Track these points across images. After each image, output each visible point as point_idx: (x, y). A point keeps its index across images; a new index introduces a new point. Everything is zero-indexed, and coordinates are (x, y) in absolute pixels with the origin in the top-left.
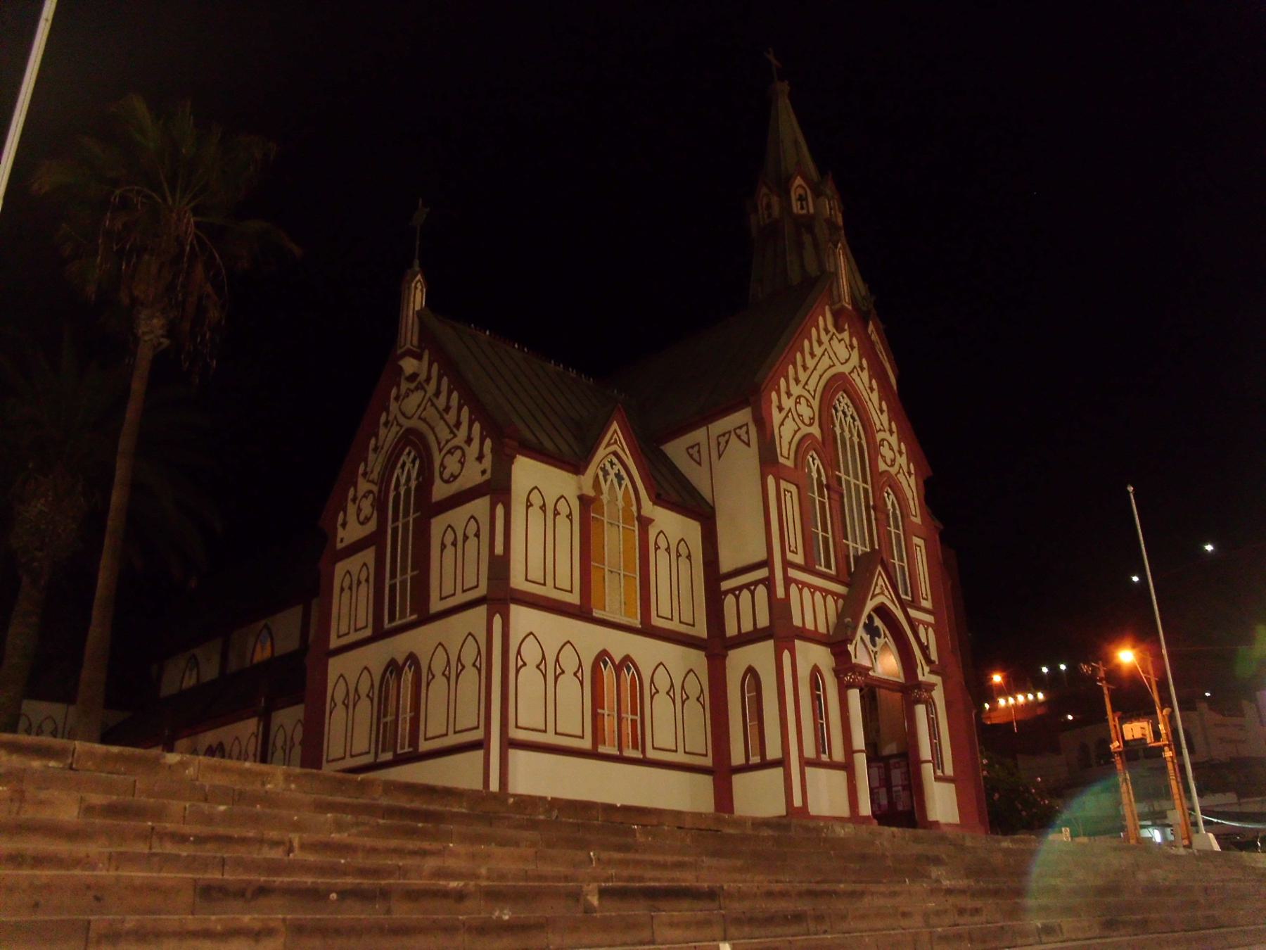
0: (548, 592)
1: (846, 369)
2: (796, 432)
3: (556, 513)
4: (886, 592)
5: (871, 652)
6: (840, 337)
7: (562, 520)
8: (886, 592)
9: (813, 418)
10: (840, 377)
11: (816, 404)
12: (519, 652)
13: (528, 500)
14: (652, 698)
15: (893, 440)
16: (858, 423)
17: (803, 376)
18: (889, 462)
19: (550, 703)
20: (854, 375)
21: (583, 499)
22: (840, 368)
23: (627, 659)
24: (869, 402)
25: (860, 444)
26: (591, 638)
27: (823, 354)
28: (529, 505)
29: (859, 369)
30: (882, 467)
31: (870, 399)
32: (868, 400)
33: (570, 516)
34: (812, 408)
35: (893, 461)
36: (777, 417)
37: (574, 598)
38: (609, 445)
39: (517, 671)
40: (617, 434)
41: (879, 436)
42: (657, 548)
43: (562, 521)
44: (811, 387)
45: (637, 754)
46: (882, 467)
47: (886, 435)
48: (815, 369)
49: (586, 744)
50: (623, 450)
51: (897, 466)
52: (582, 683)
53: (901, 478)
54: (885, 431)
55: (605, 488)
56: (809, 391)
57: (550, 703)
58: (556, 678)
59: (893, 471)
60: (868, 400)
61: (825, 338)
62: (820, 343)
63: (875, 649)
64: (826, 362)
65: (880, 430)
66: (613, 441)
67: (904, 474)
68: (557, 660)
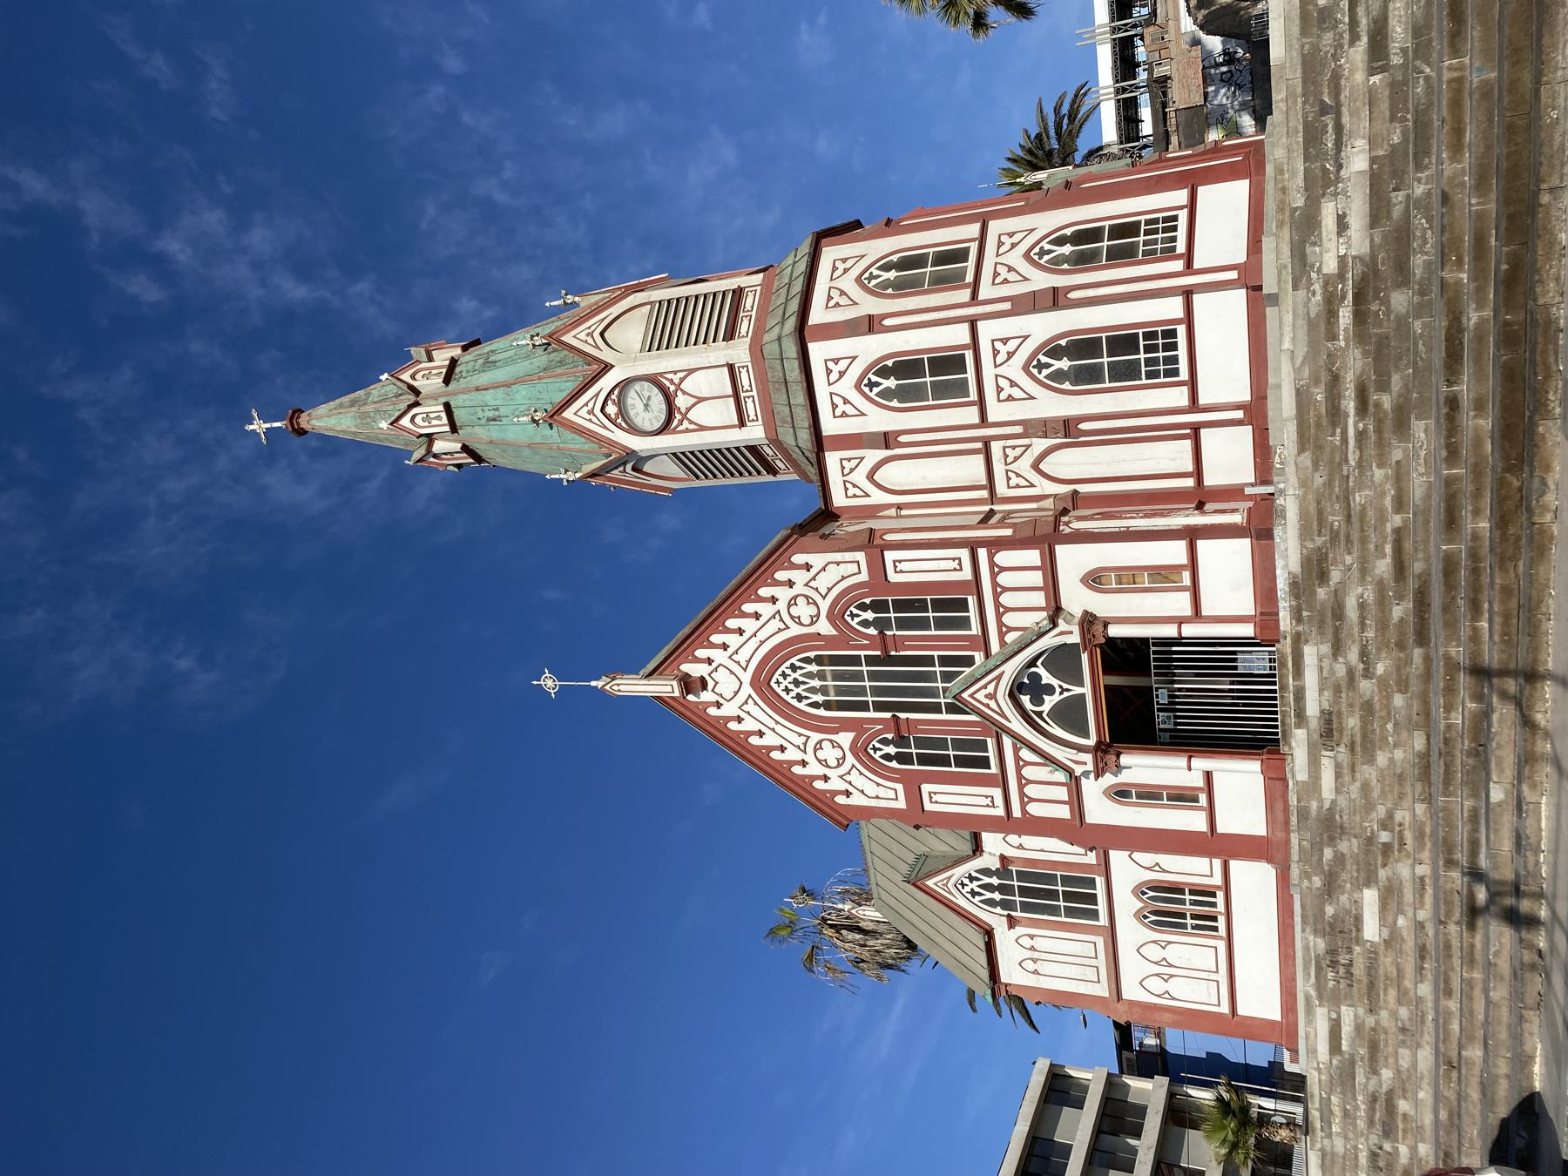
0: (1102, 962)
1: (747, 677)
2: (861, 773)
3: (1032, 949)
4: (991, 688)
5: (1062, 697)
6: (711, 684)
7: (1038, 943)
8: (991, 688)
9: (831, 741)
10: (755, 683)
11: (816, 737)
12: (1159, 996)
13: (1033, 973)
14: (1165, 871)
15: (783, 594)
16: (793, 660)
17: (792, 754)
18: (813, 610)
19: (1192, 974)
20: (742, 657)
21: (1012, 922)
22: (747, 690)
23: (1139, 891)
24: (761, 636)
25: (819, 660)
26: (1131, 932)
28: (1036, 972)
29: (730, 651)
30: (824, 627)
32: (754, 643)
33: (1032, 937)
34: (820, 742)
35: (810, 601)
36: (857, 800)
37: (1100, 941)
38: (950, 893)
39: (1174, 999)
40: (939, 882)
41: (795, 630)
42: (1021, 847)
43: (1038, 943)
44: (800, 741)
45: (1220, 895)
46: (824, 627)
47: (782, 605)
48: (773, 730)
49: (1222, 945)
50: (949, 878)
52: (1170, 943)
53: (823, 582)
55: (988, 895)
56: (805, 744)
57: (1192, 974)
58: (1171, 966)
59: (825, 606)
60: (754, 643)
61: (729, 710)
62: (739, 720)
63: (1058, 690)
64: (750, 707)
65: (781, 620)
66: (946, 888)
68: (1156, 963)
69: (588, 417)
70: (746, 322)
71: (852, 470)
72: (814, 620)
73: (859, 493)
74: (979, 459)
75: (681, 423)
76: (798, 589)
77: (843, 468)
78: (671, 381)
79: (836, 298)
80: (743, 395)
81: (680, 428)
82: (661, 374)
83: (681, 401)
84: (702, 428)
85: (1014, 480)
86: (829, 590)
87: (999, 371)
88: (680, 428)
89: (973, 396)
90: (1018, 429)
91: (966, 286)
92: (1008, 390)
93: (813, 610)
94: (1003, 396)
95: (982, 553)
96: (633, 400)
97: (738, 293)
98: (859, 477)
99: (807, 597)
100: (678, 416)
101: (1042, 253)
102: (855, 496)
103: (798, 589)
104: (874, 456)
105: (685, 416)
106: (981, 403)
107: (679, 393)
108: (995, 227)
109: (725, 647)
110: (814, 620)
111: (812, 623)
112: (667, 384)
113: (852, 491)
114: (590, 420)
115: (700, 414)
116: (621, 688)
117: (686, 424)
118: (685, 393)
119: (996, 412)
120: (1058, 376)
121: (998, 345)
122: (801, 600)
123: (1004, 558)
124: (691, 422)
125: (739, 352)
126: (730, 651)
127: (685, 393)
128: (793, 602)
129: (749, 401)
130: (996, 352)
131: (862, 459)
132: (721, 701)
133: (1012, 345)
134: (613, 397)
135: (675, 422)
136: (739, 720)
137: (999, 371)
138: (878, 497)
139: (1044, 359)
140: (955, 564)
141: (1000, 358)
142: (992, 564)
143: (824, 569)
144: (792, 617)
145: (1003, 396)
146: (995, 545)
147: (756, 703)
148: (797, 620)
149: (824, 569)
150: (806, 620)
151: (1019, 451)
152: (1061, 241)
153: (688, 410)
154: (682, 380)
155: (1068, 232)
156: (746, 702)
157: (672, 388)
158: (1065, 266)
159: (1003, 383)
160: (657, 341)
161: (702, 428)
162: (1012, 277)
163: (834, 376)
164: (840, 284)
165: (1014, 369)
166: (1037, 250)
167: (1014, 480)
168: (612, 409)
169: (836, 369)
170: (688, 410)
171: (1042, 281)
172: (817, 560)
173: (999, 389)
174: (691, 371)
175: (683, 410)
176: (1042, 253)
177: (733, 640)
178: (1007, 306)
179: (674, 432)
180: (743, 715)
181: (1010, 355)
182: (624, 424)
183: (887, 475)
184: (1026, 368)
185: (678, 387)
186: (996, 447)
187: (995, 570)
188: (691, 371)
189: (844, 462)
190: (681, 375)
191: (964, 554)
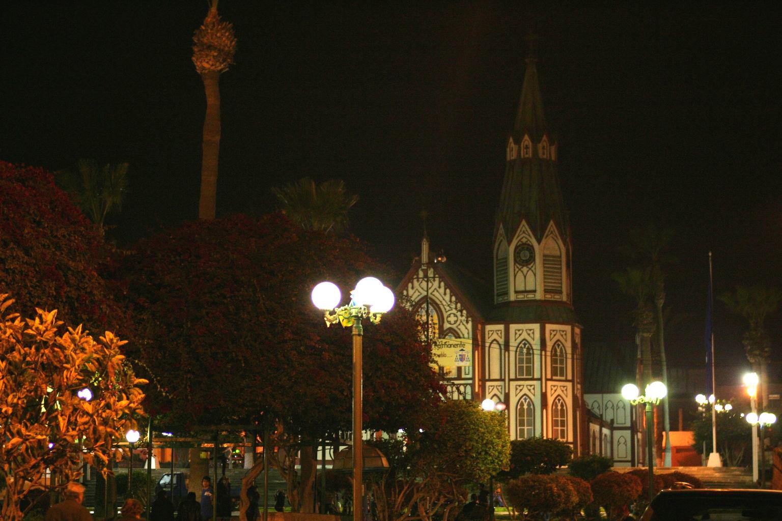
18: (452, 322)
20: (435, 293)
27: (415, 292)
29: (438, 289)
30: (447, 326)
31: (444, 299)
41: (445, 315)
46: (447, 326)
51: (458, 323)
53: (462, 327)
54: (452, 310)
59: (454, 326)
60: (441, 299)
62: (413, 288)
64: (417, 294)
65: (449, 310)
67: (463, 324)
69: (522, 230)
70: (550, 296)
71: (498, 334)
72: (449, 322)
73: (490, 334)
74: (498, 377)
75: (518, 267)
76: (460, 318)
77: (499, 331)
78: (532, 267)
79: (553, 333)
80: (525, 294)
81: (516, 267)
82: (535, 263)
83: (525, 269)
84: (515, 276)
85: (491, 388)
86: (459, 329)
87: (525, 386)
88: (516, 267)
89: (518, 377)
90: (507, 391)
91: (552, 376)
92: (519, 388)
93: (452, 322)
94: (518, 387)
95: (470, 382)
96: (527, 253)
97: (560, 292)
98: (495, 336)
99: (457, 321)
100: (520, 267)
101: (559, 400)
102: (489, 334)
103: (460, 318)
104: (502, 341)
105: (520, 270)
106: (516, 379)
107: (528, 269)
108: (569, 385)
109: (440, 287)
110: (449, 322)
111: (448, 321)
112: (532, 265)
113: (491, 333)
114: (521, 231)
115: (520, 276)
116: (425, 246)
117: (517, 270)
118: (528, 271)
119: (513, 384)
120: (522, 405)
121: (533, 387)
122: (456, 319)
123: (469, 389)
124: (518, 272)
125: (539, 296)
126: (438, 289)
127: (528, 271)
128: (455, 316)
129: (523, 296)
130: (531, 386)
131: (501, 338)
132: (419, 282)
133: (532, 391)
134: (529, 242)
135: (518, 266)
136: (413, 288)
137: (525, 386)
138: (488, 341)
139: (527, 401)
140: (467, 373)
141: (529, 387)
142: (467, 384)
143: (466, 328)
144: (450, 314)
145: (518, 387)
146: (473, 386)
147: (419, 296)
148: (449, 316)
149: (466, 328)
150: (449, 319)
151: (500, 390)
152: (562, 406)
153: (522, 272)
154: (532, 271)
155: (565, 408)
156: (419, 292)
157: (530, 266)
158: (554, 407)
159: (521, 387)
160: (546, 258)
161: (515, 276)
162: (553, 391)
163: (529, 332)
164: (558, 334)
165: (525, 391)
166: (560, 398)
167: (491, 388)
168: (524, 240)
169: (531, 332)
170: (522, 272)
171: (550, 400)
172: (470, 326)
173: (520, 386)
174: (535, 275)
175: (522, 269)
176: (559, 400)
177: (442, 290)
178: (544, 391)
179: (515, 264)
180: (415, 289)
181: (530, 390)
182: (518, 244)
183: (495, 345)
184: (525, 395)
185: (530, 269)
186: (501, 383)
187: (465, 385)
188: (535, 275)
189: (500, 332)
190: (534, 271)
191: (470, 376)
